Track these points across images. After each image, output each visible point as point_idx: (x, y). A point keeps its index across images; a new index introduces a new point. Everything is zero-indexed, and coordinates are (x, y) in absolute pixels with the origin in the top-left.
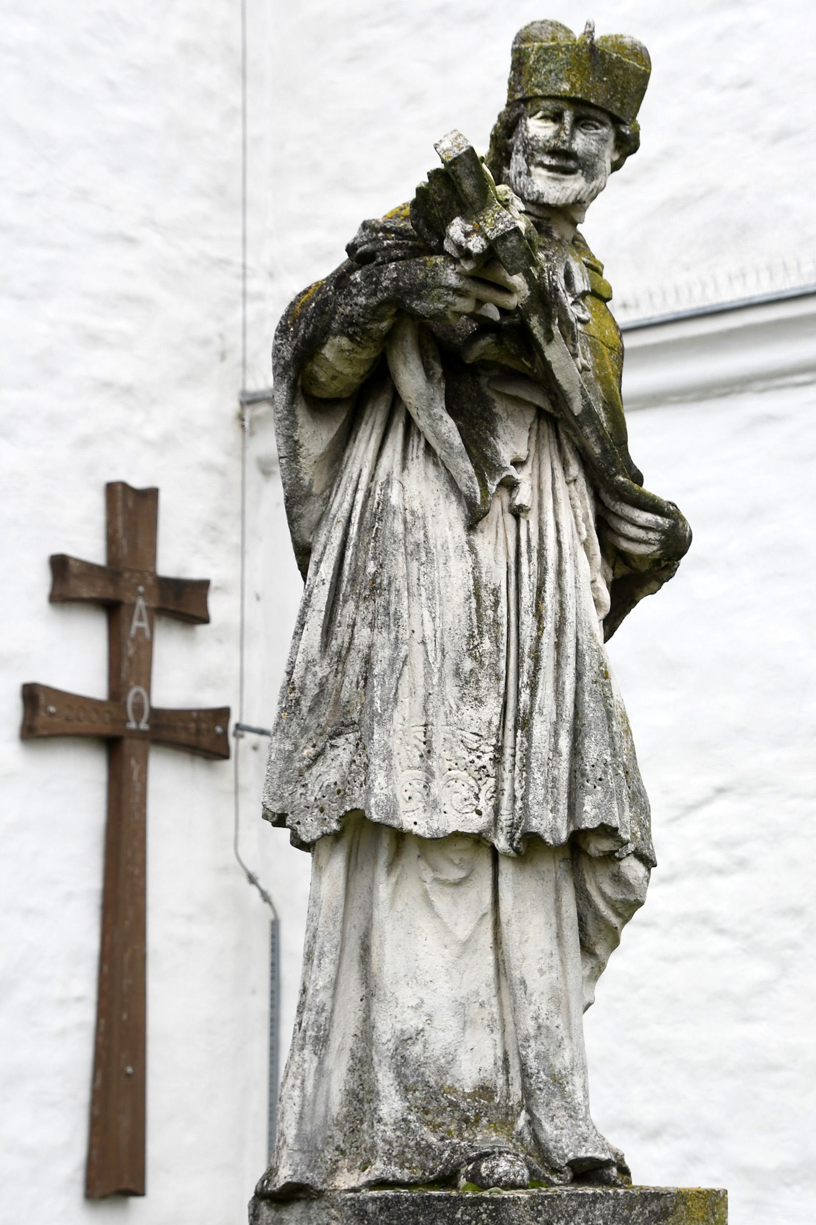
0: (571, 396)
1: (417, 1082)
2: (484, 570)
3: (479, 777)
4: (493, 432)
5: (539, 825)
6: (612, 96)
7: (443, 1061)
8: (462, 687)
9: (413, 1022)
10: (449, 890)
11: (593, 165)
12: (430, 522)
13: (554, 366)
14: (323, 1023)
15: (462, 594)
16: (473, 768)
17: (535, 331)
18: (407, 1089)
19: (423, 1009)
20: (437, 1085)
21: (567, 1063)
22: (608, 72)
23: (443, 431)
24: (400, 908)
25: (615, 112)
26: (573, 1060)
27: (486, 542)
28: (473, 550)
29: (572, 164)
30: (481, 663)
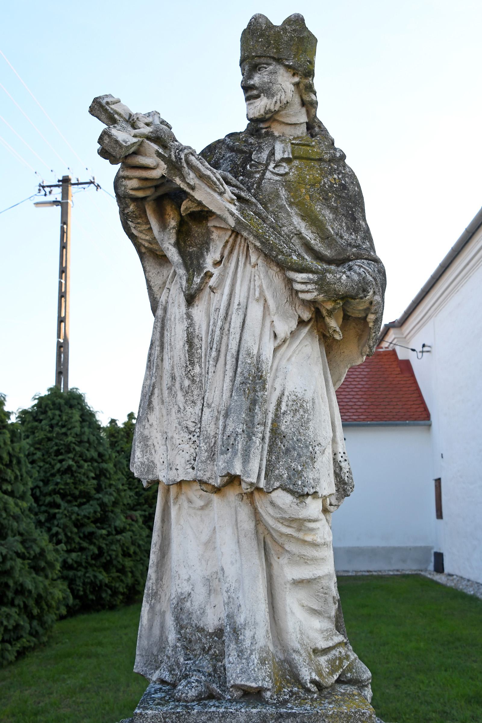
0: (224, 217)
1: (187, 623)
2: (197, 328)
3: (194, 447)
4: (208, 250)
5: (202, 475)
6: (267, 48)
7: (198, 612)
8: (184, 396)
9: (186, 588)
10: (199, 512)
11: (269, 89)
12: (169, 307)
13: (204, 203)
14: (151, 586)
15: (181, 343)
16: (191, 442)
17: (182, 186)
18: (182, 628)
19: (190, 581)
20: (196, 626)
21: (242, 621)
22: (262, 35)
23: (170, 255)
24: (182, 522)
25: (272, 55)
26: (245, 620)
27: (199, 311)
28: (189, 316)
29: (255, 92)
30: (193, 381)
